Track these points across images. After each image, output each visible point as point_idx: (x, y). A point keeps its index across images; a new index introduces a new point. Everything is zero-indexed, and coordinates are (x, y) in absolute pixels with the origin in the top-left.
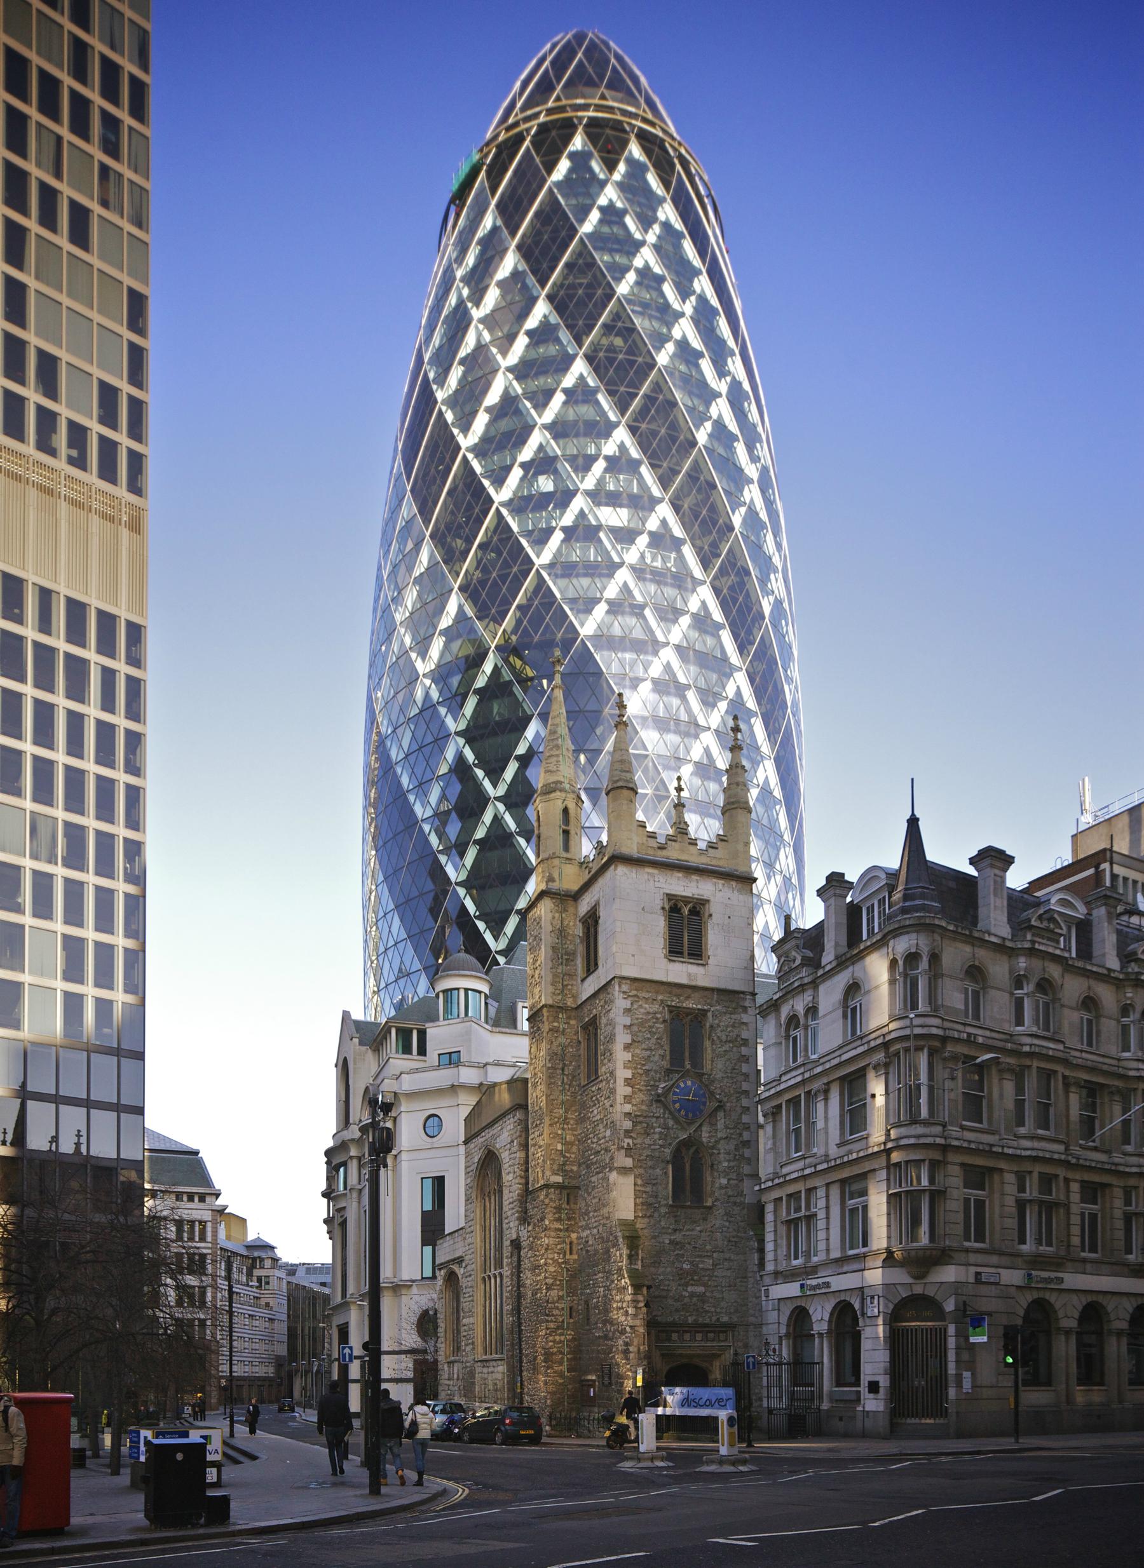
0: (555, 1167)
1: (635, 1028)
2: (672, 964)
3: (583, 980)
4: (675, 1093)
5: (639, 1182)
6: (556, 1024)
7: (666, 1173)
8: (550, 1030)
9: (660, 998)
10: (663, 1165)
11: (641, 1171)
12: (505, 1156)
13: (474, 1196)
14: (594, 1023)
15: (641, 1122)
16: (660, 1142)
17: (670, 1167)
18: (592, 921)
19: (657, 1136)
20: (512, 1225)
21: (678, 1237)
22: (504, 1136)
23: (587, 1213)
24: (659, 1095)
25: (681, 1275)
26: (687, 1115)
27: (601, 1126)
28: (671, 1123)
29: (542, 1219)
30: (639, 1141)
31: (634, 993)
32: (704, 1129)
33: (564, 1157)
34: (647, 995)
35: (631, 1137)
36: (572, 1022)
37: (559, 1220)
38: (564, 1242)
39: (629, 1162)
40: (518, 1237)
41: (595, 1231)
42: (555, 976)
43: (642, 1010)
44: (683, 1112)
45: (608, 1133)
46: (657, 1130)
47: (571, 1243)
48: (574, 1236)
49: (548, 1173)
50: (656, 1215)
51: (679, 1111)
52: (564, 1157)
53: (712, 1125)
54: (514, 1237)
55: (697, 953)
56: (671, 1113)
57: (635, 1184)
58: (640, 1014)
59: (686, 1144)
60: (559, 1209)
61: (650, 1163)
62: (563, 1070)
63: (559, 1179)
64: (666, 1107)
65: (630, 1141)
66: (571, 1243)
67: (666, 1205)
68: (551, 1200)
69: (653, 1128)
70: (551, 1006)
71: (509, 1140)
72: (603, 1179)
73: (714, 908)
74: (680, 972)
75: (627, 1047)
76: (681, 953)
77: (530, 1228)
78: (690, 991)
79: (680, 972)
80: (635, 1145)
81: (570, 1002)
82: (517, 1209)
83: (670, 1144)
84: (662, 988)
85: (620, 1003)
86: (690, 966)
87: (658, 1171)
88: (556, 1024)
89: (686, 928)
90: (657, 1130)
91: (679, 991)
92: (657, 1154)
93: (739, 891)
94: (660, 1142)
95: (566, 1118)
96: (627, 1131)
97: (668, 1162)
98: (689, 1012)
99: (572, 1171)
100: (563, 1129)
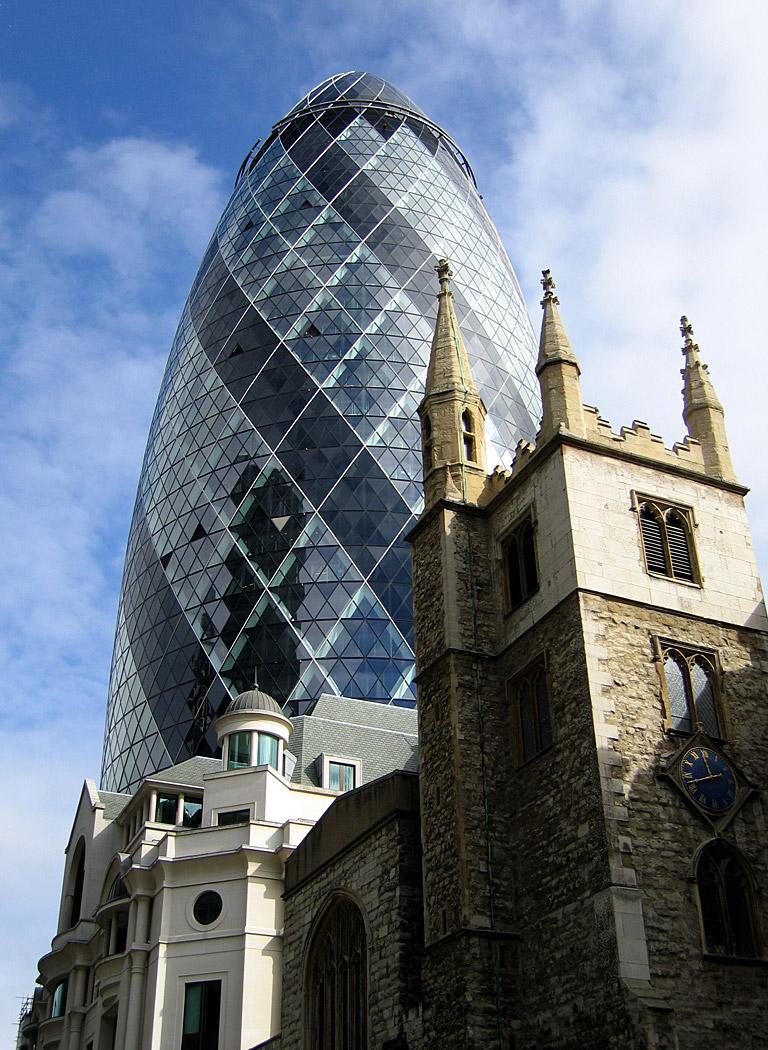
0: (478, 900)
1: (614, 665)
2: (655, 582)
3: (506, 617)
4: (687, 769)
5: (651, 913)
6: (467, 678)
7: (690, 900)
8: (461, 685)
9: (646, 625)
10: (683, 885)
11: (652, 893)
12: (370, 902)
13: (302, 979)
14: (539, 670)
15: (640, 811)
16: (675, 846)
17: (696, 889)
19: (667, 836)
20: (386, 1013)
21: (726, 1017)
22: (367, 878)
23: (542, 978)
24: (663, 769)
26: (709, 803)
27: (564, 824)
28: (686, 815)
29: (460, 991)
30: (640, 841)
31: (605, 614)
32: (737, 828)
33: (492, 884)
34: (627, 620)
35: (628, 834)
36: (492, 678)
37: (488, 994)
38: (500, 1036)
40: (402, 1032)
41: (567, 1010)
42: (463, 611)
43: (622, 640)
44: (702, 799)
45: (583, 831)
46: (667, 825)
47: (512, 1039)
48: (515, 1024)
49: (466, 911)
50: (685, 974)
51: (696, 796)
52: (492, 884)
53: (749, 823)
54: (393, 1033)
55: (689, 573)
56: (684, 799)
57: (645, 916)
58: (620, 645)
59: (713, 853)
60: (487, 973)
61: (662, 881)
62: (482, 746)
64: (673, 787)
65: (628, 840)
66: (512, 1039)
67: (697, 957)
68: (474, 957)
69: (659, 820)
70: (460, 652)
71: (380, 870)
72: (576, 911)
73: (699, 516)
74: (667, 593)
75: (606, 691)
76: (665, 572)
77: (429, 1014)
78: (684, 621)
80: (636, 847)
81: (486, 649)
82: (398, 983)
83: (690, 851)
84: (645, 613)
85: (590, 627)
86: (679, 587)
87: (676, 897)
88: (467, 678)
90: (667, 825)
91: (670, 619)
92: (671, 866)
93: (727, 501)
94: (675, 846)
95: (490, 822)
96: (622, 824)
97: (690, 881)
99: (505, 908)
100: (486, 837)
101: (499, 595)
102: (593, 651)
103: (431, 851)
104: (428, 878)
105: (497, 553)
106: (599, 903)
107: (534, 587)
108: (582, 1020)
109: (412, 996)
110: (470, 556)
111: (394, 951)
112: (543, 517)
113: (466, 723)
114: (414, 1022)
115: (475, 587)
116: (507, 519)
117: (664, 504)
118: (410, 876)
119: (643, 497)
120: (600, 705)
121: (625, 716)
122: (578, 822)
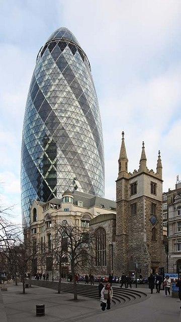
14: (135, 204)
18: (135, 184)
25: (153, 252)
39: (146, 231)
63: (125, 233)
73: (158, 185)
79: (152, 196)
85: (145, 201)
89: (154, 187)
98: (154, 204)
101: (129, 193)
102: (145, 204)
103: (117, 224)
104: (117, 227)
105: (129, 186)
106: (142, 233)
107: (136, 193)
108: (137, 245)
109: (114, 240)
110: (126, 186)
111: (111, 235)
112: (138, 183)
113: (125, 210)
114: (114, 243)
115: (126, 191)
116: (132, 182)
117: (154, 183)
118: (114, 226)
119: (152, 182)
120: (145, 211)
121: (146, 212)
122: (139, 224)
